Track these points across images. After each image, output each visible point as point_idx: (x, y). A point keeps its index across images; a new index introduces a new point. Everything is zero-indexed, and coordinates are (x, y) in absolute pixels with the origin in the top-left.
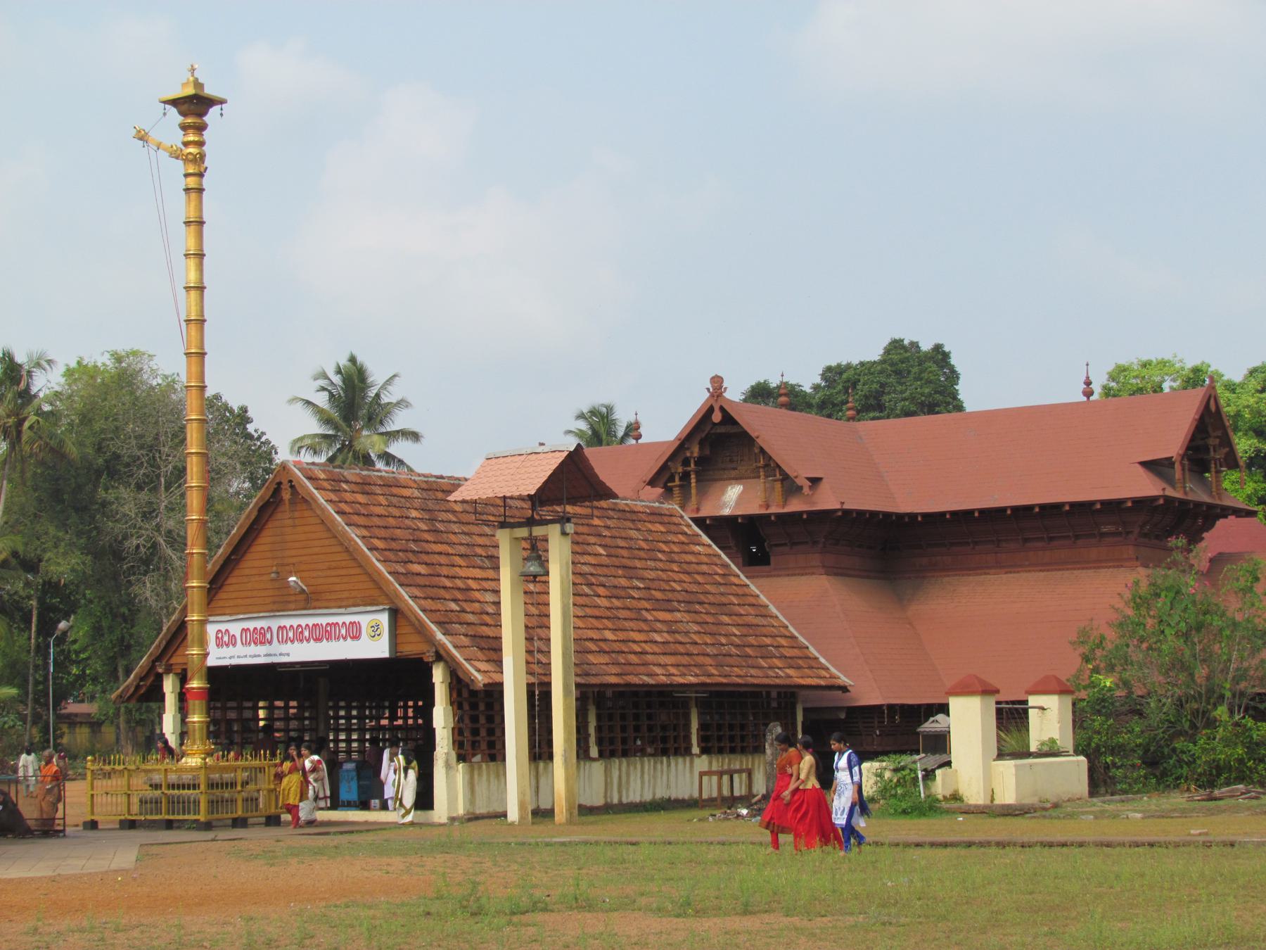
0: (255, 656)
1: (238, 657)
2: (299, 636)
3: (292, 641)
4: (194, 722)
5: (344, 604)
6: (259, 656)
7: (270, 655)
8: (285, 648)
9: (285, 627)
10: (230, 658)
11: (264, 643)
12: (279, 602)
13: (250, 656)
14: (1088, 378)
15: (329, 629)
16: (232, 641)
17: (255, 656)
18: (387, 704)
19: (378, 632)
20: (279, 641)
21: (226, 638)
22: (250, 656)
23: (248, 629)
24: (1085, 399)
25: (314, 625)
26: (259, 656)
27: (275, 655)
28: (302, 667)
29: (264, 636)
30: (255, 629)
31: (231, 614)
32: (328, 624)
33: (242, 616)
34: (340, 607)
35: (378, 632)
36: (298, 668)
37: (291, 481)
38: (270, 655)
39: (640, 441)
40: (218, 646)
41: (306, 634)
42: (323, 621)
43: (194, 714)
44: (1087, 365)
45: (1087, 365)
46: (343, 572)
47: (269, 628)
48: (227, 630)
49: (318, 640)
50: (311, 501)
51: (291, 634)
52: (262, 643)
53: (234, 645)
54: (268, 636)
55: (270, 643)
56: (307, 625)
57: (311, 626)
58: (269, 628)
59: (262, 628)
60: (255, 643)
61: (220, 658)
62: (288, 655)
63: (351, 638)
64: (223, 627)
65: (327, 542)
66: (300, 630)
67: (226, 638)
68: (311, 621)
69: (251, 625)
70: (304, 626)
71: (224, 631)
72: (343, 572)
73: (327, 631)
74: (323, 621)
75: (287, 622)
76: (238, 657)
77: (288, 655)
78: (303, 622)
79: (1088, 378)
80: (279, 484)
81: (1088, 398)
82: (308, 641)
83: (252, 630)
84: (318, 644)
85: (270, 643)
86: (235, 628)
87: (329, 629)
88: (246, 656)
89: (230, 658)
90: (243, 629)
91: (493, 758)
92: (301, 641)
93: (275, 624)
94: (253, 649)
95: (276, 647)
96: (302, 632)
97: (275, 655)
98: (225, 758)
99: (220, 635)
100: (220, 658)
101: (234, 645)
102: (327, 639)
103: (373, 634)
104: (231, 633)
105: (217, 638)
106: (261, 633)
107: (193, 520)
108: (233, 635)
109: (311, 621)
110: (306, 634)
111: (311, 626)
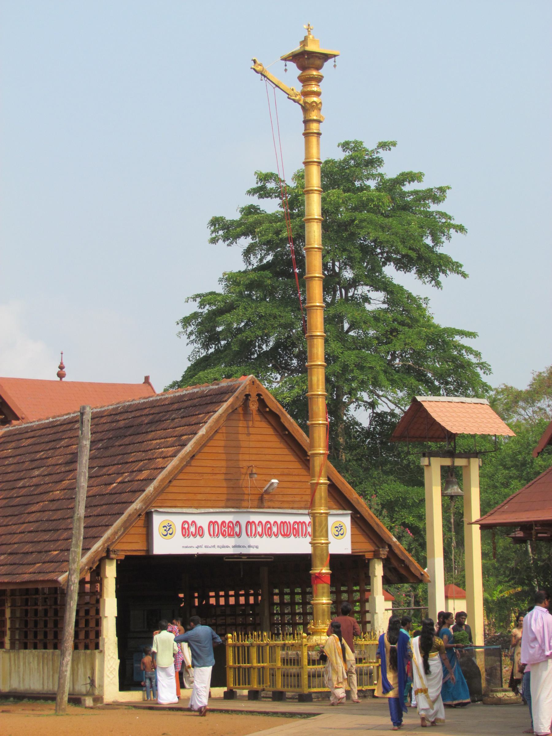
0: (223, 547)
1: (206, 547)
2: (267, 531)
3: (261, 536)
4: (323, 604)
5: (295, 506)
6: (227, 547)
7: (239, 547)
8: (253, 541)
9: (253, 522)
10: (198, 547)
11: (233, 535)
12: (233, 500)
13: (218, 546)
14: (62, 363)
15: (296, 526)
16: (199, 532)
17: (223, 547)
18: (196, 595)
19: (170, 532)
20: (248, 535)
21: (192, 529)
22: (205, 547)
23: (216, 522)
24: (58, 379)
25: (282, 522)
26: (227, 547)
27: (244, 547)
28: (248, 558)
29: (233, 529)
30: (223, 522)
31: (197, 508)
32: (295, 522)
33: (218, 510)
34: (292, 508)
35: (170, 532)
36: (244, 559)
37: (259, 395)
38: (239, 547)
39: (64, 379)
40: (184, 535)
41: (275, 529)
42: (291, 519)
43: (323, 596)
44: (62, 354)
45: (62, 354)
46: (297, 478)
47: (238, 522)
48: (193, 522)
49: (285, 535)
50: (280, 415)
51: (259, 529)
52: (229, 535)
53: (202, 536)
54: (237, 529)
55: (239, 535)
56: (275, 522)
57: (279, 523)
58: (238, 522)
59: (230, 522)
60: (224, 535)
61: (187, 547)
62: (257, 547)
63: (282, 535)
64: (190, 519)
65: (278, 451)
66: (269, 526)
67: (192, 529)
68: (279, 519)
69: (220, 519)
70: (272, 523)
71: (190, 522)
72: (297, 478)
73: (294, 528)
74: (291, 519)
75: (255, 518)
76: (206, 547)
77: (257, 547)
78: (272, 519)
79: (62, 363)
80: (247, 396)
81: (61, 378)
82: (276, 536)
83: (220, 523)
84: (286, 539)
85: (239, 535)
86: (203, 521)
87: (296, 526)
88: (214, 546)
89: (198, 547)
90: (211, 522)
91: (55, 647)
92: (270, 535)
93: (243, 519)
94: (221, 541)
95: (244, 539)
96: (270, 528)
97: (244, 547)
98: (260, 638)
99: (186, 526)
100: (187, 547)
101: (202, 536)
102: (295, 536)
103: (165, 533)
104: (198, 525)
105: (183, 528)
106: (229, 527)
107: (320, 424)
108: (201, 527)
109: (279, 519)
110: (275, 529)
111: (279, 523)
